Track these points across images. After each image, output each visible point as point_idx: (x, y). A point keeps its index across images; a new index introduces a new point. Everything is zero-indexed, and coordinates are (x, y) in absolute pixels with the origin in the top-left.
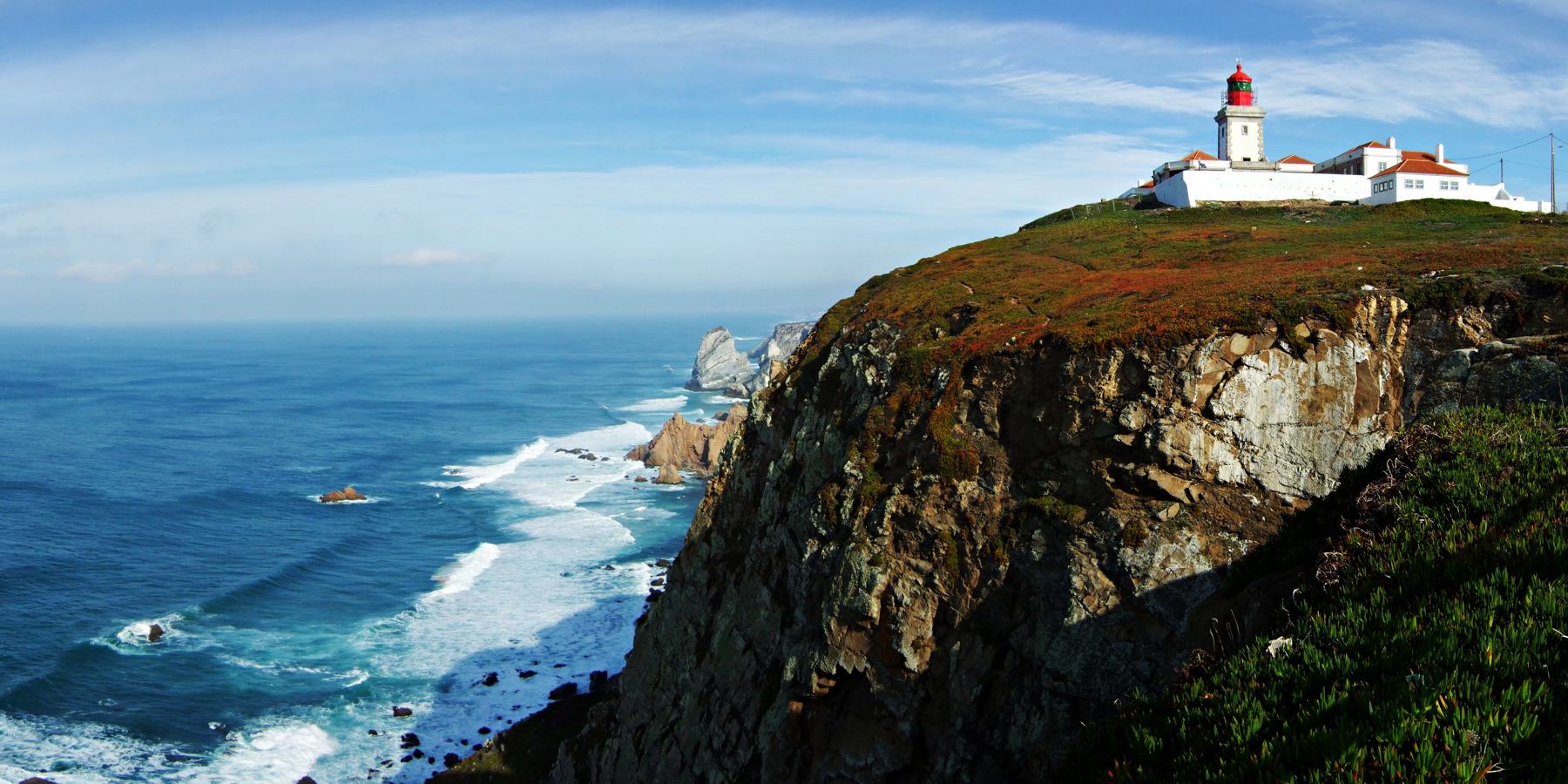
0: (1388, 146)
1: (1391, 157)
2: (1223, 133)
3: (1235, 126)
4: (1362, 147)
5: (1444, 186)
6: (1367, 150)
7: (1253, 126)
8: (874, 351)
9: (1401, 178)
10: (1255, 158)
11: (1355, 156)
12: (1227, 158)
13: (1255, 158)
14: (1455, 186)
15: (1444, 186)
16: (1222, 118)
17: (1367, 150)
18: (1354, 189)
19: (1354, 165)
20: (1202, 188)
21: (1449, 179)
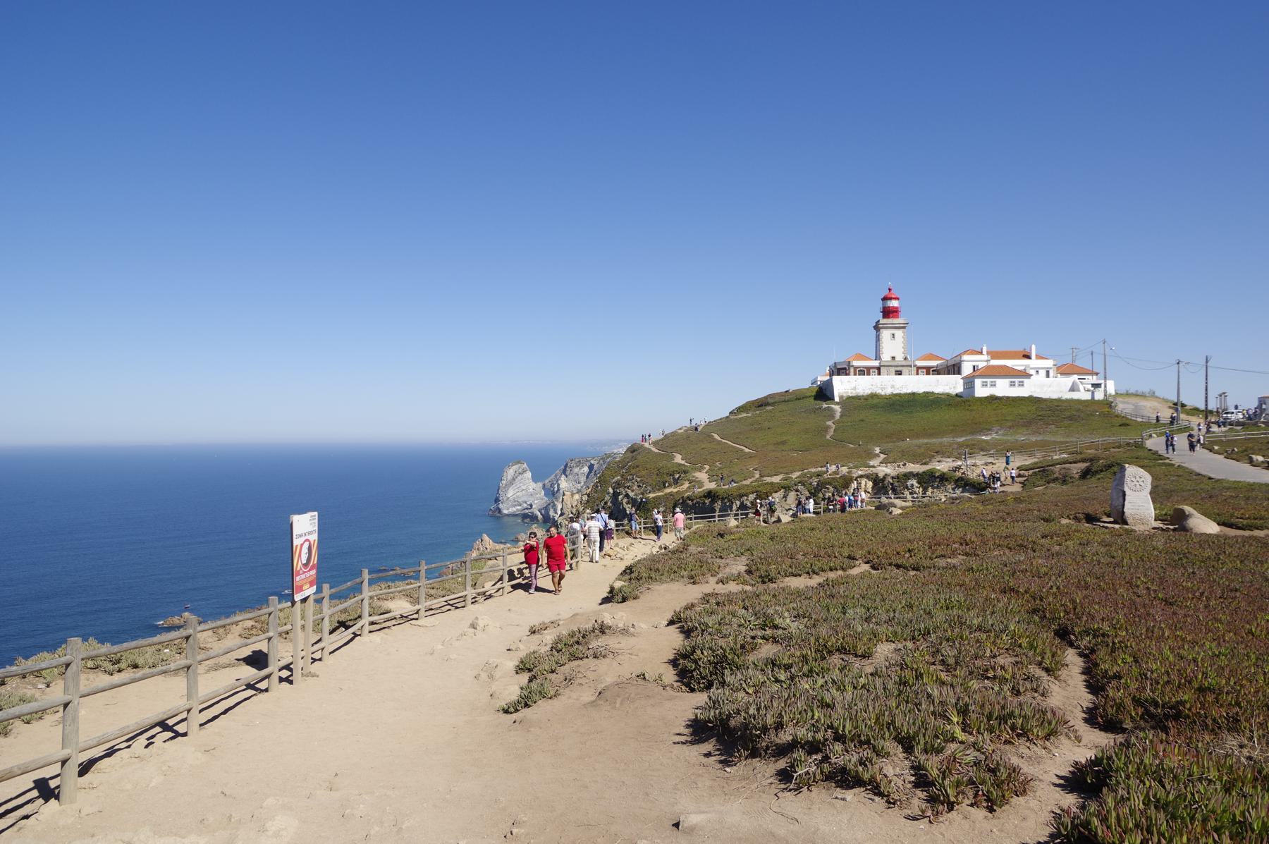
0: (981, 353)
1: (982, 361)
2: (878, 339)
3: (885, 334)
4: (960, 355)
5: (1012, 384)
6: (965, 357)
7: (899, 333)
8: (631, 494)
9: (978, 382)
10: (900, 358)
11: (957, 359)
12: (877, 357)
13: (900, 358)
14: (1021, 384)
15: (1012, 384)
16: (877, 327)
17: (965, 357)
18: (950, 385)
19: (954, 369)
20: (843, 386)
21: (1017, 380)
